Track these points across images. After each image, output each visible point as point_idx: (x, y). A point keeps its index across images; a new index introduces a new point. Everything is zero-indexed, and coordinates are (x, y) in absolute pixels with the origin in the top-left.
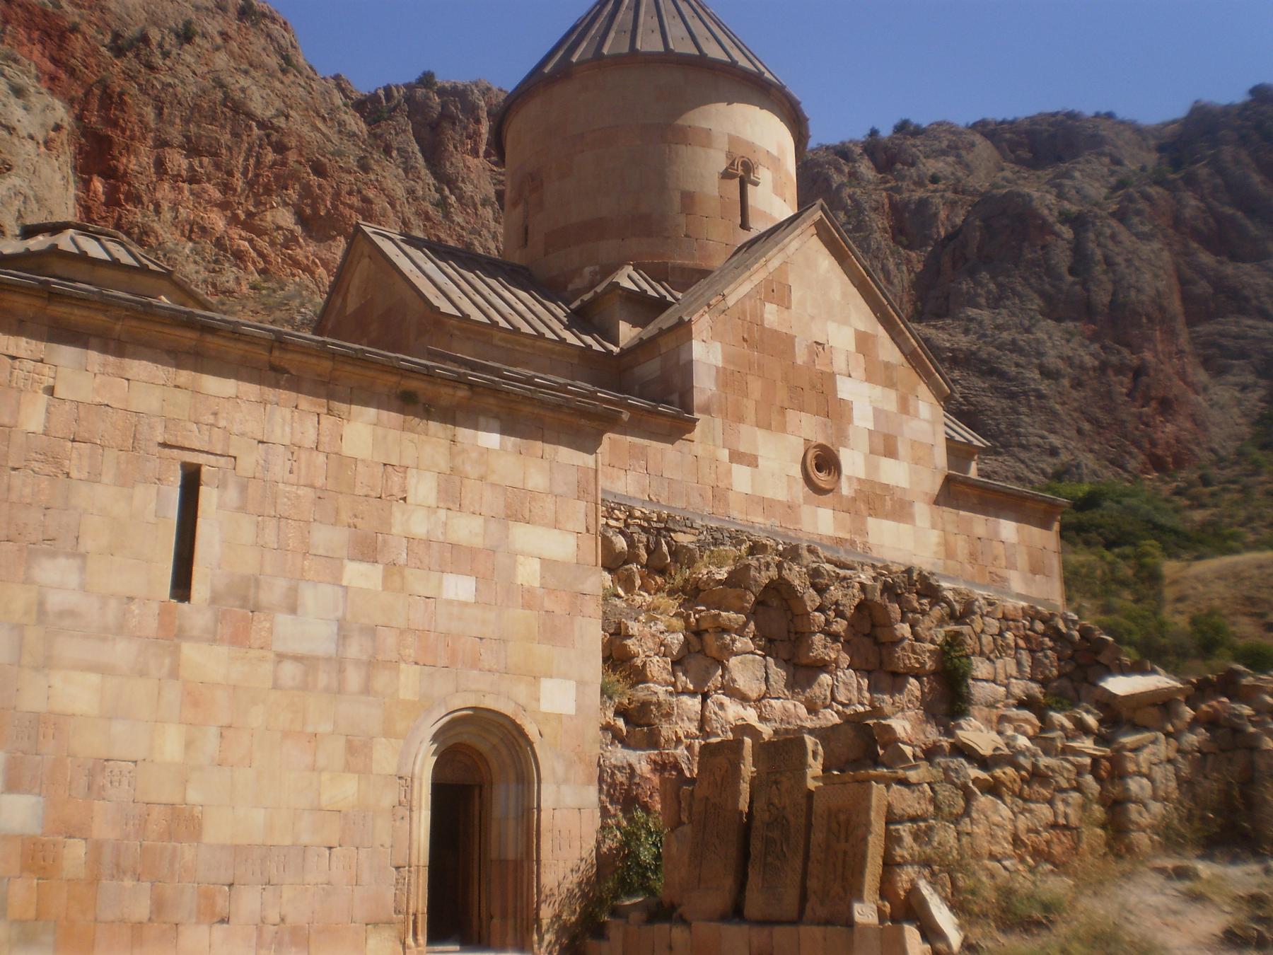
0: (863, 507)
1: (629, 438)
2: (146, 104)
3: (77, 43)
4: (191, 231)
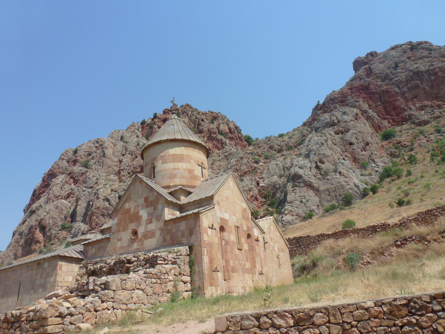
0: (143, 239)
1: (102, 245)
2: (395, 88)
3: (372, 86)
4: (422, 108)
